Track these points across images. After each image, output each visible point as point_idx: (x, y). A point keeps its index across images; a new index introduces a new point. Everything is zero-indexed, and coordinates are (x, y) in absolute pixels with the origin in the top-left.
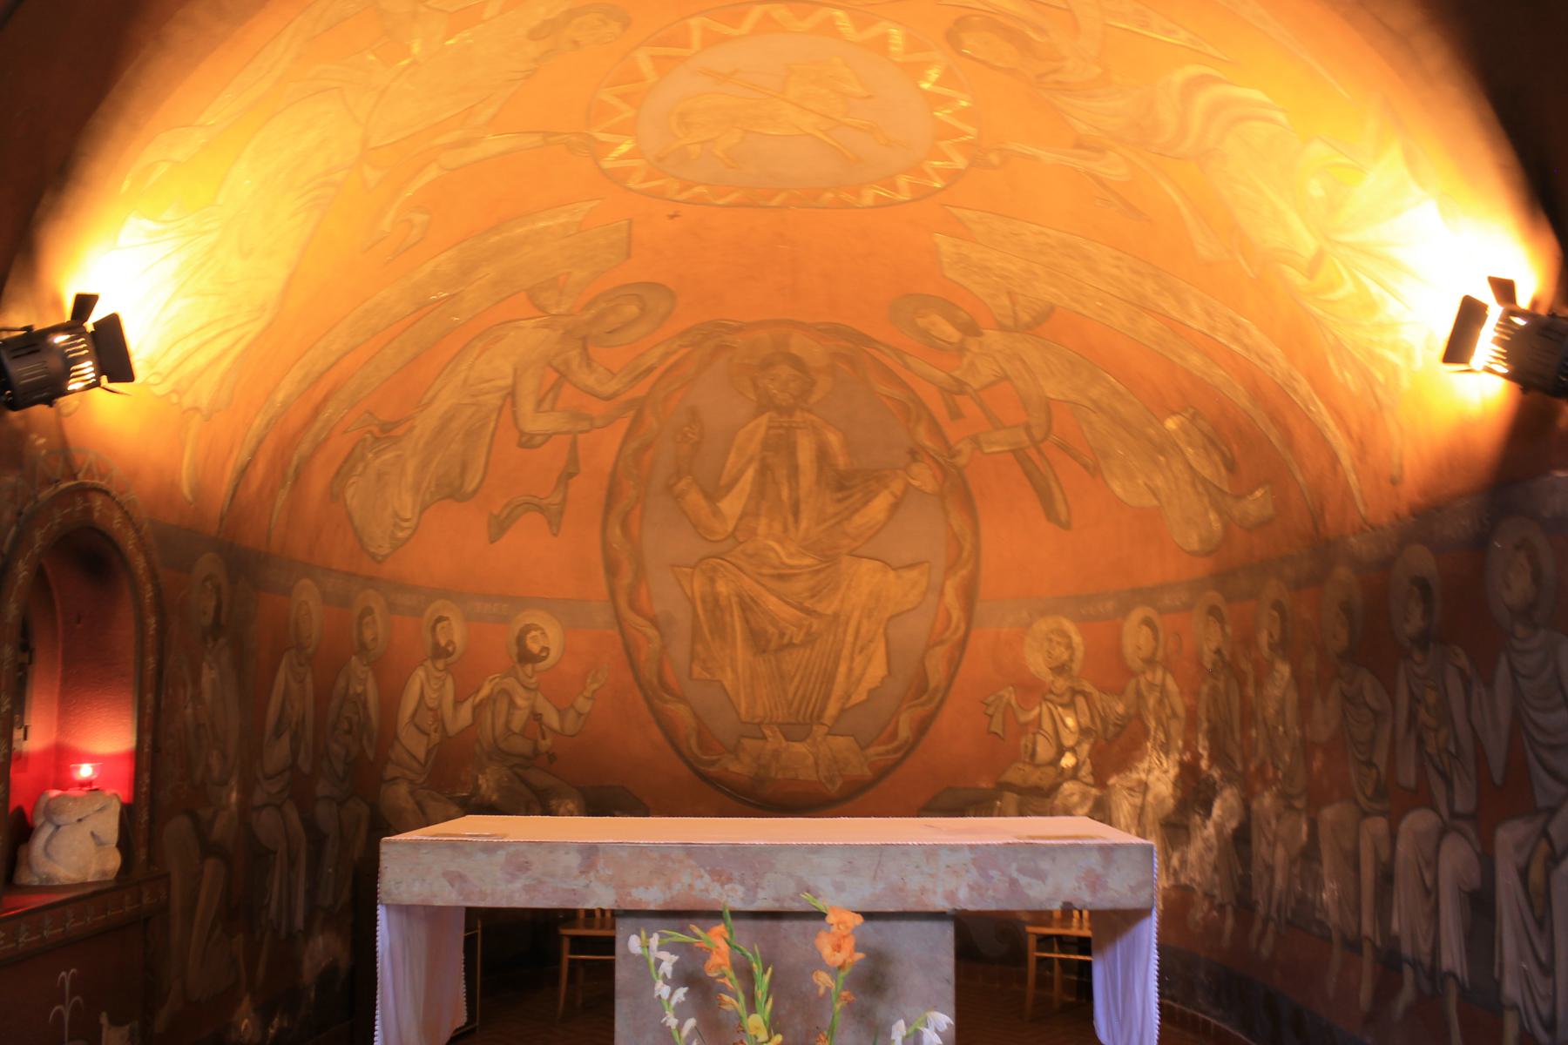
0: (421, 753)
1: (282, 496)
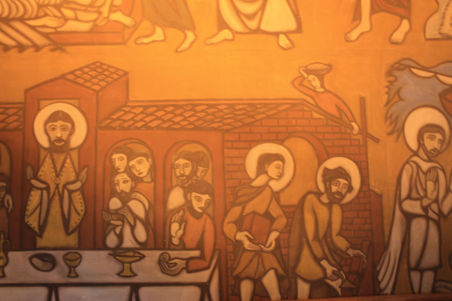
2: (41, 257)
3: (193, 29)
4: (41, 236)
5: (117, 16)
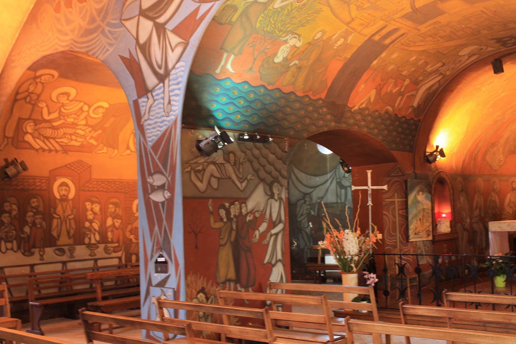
0: (511, 212)
1: (472, 163)
2: (58, 249)
3: (117, 149)
4: (58, 240)
5: (92, 141)
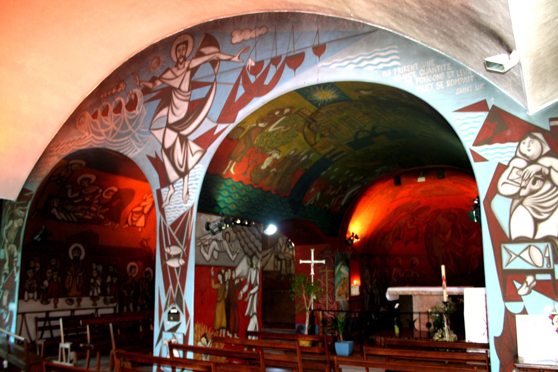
3: (119, 223)
5: (102, 217)
